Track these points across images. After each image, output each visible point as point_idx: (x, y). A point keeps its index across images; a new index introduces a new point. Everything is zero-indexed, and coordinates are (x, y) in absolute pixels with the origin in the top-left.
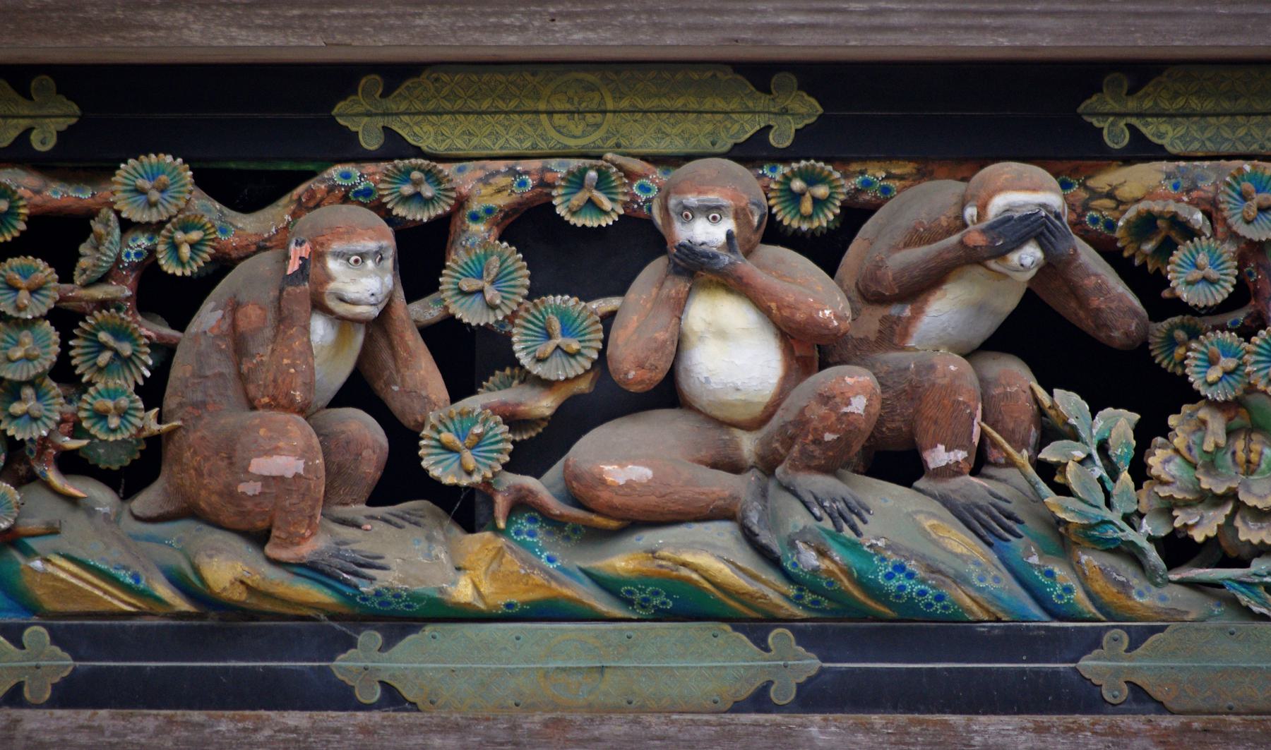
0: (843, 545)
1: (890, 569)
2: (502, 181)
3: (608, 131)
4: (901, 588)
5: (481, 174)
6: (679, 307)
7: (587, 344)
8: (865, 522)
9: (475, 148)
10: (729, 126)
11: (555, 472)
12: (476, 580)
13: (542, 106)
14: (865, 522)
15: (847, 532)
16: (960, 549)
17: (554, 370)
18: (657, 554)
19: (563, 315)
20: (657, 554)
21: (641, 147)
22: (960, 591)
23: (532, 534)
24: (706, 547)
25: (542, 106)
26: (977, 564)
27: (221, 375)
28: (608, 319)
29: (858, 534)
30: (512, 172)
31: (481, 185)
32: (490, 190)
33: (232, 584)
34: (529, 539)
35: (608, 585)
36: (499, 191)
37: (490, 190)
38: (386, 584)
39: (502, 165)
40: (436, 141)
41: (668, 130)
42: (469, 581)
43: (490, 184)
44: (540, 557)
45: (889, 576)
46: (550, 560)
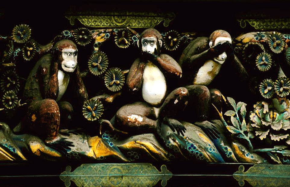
0: (179, 138)
1: (190, 146)
2: (103, 35)
3: (127, 22)
4: (192, 152)
5: (98, 33)
6: (142, 70)
7: (121, 82)
8: (185, 132)
9: (96, 26)
10: (154, 20)
11: (113, 119)
12: (94, 150)
13: (112, 14)
14: (185, 132)
15: (181, 135)
16: (205, 141)
17: (113, 89)
18: (136, 142)
19: (116, 73)
20: (136, 142)
21: (134, 26)
22: (205, 153)
23: (107, 137)
24: (147, 140)
25: (112, 14)
26: (210, 145)
27: (36, 89)
28: (126, 75)
29: (183, 135)
30: (105, 32)
31: (98, 36)
32: (100, 37)
33: (37, 151)
34: (106, 138)
35: (124, 151)
36: (102, 38)
37: (100, 37)
38: (73, 151)
39: (103, 31)
40: (88, 23)
41: (141, 22)
42: (92, 150)
43: (100, 36)
44: (109, 144)
45: (190, 148)
46: (111, 144)
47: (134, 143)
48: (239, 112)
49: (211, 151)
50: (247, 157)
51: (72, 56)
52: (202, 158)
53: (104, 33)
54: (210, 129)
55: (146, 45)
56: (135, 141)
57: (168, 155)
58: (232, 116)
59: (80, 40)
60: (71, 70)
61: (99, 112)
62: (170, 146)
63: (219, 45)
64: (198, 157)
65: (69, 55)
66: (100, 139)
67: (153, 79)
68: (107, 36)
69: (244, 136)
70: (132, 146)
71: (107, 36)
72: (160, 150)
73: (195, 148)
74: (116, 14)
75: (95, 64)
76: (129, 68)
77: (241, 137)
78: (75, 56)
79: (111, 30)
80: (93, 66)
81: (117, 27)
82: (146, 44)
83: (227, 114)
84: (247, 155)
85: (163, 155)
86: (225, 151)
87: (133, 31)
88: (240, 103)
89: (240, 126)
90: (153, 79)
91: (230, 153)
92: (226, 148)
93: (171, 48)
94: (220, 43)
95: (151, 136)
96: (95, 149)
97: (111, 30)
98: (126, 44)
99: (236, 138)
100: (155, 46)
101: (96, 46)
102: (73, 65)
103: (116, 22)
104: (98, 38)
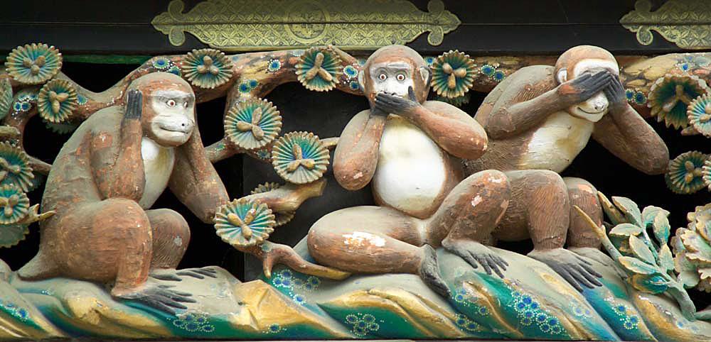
2: (262, 64)
3: (327, 35)
4: (529, 314)
5: (248, 60)
13: (286, 19)
16: (563, 292)
17: (298, 178)
22: (565, 319)
28: (332, 149)
30: (268, 58)
31: (248, 66)
32: (254, 69)
34: (285, 286)
37: (254, 69)
38: (194, 312)
39: (261, 55)
42: (248, 311)
43: (254, 66)
47: (365, 295)
48: (650, 230)
49: (579, 315)
50: (680, 328)
51: (180, 106)
52: (556, 329)
53: (264, 59)
54: (574, 267)
55: (384, 81)
56: (368, 291)
57: (461, 322)
58: (631, 236)
59: (201, 75)
60: (179, 136)
61: (262, 226)
62: (466, 301)
63: (585, 78)
64: (546, 327)
65: (172, 104)
66: (267, 286)
67: (407, 154)
68: (275, 65)
69: (668, 281)
70: (359, 300)
71: (275, 65)
72: (440, 311)
73: (535, 306)
74: (296, 19)
75: (244, 124)
76: (338, 134)
77: (661, 282)
78: (187, 106)
79: (284, 53)
80: (239, 131)
81: (301, 46)
82: (383, 77)
83: (618, 230)
84: (681, 325)
85: (445, 320)
86: (621, 314)
87: (347, 57)
88: (650, 209)
89: (657, 260)
90: (407, 154)
91: (634, 320)
92: (622, 309)
93: (452, 90)
94: (588, 73)
95: (412, 281)
96: (256, 308)
97: (284, 53)
98: (328, 82)
99: (649, 284)
100: (410, 82)
101: (244, 89)
102: (183, 125)
103: (299, 37)
104: (248, 70)
